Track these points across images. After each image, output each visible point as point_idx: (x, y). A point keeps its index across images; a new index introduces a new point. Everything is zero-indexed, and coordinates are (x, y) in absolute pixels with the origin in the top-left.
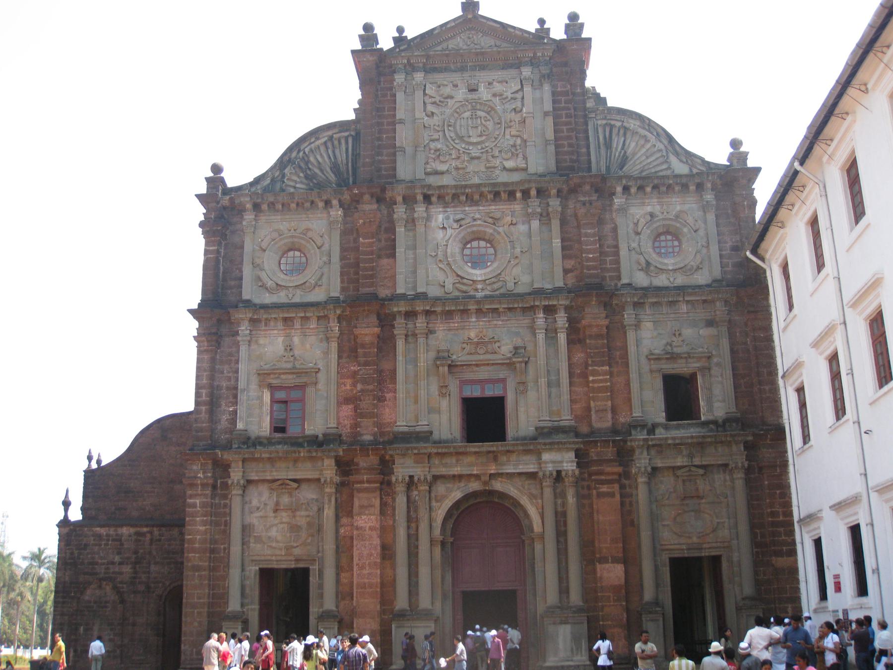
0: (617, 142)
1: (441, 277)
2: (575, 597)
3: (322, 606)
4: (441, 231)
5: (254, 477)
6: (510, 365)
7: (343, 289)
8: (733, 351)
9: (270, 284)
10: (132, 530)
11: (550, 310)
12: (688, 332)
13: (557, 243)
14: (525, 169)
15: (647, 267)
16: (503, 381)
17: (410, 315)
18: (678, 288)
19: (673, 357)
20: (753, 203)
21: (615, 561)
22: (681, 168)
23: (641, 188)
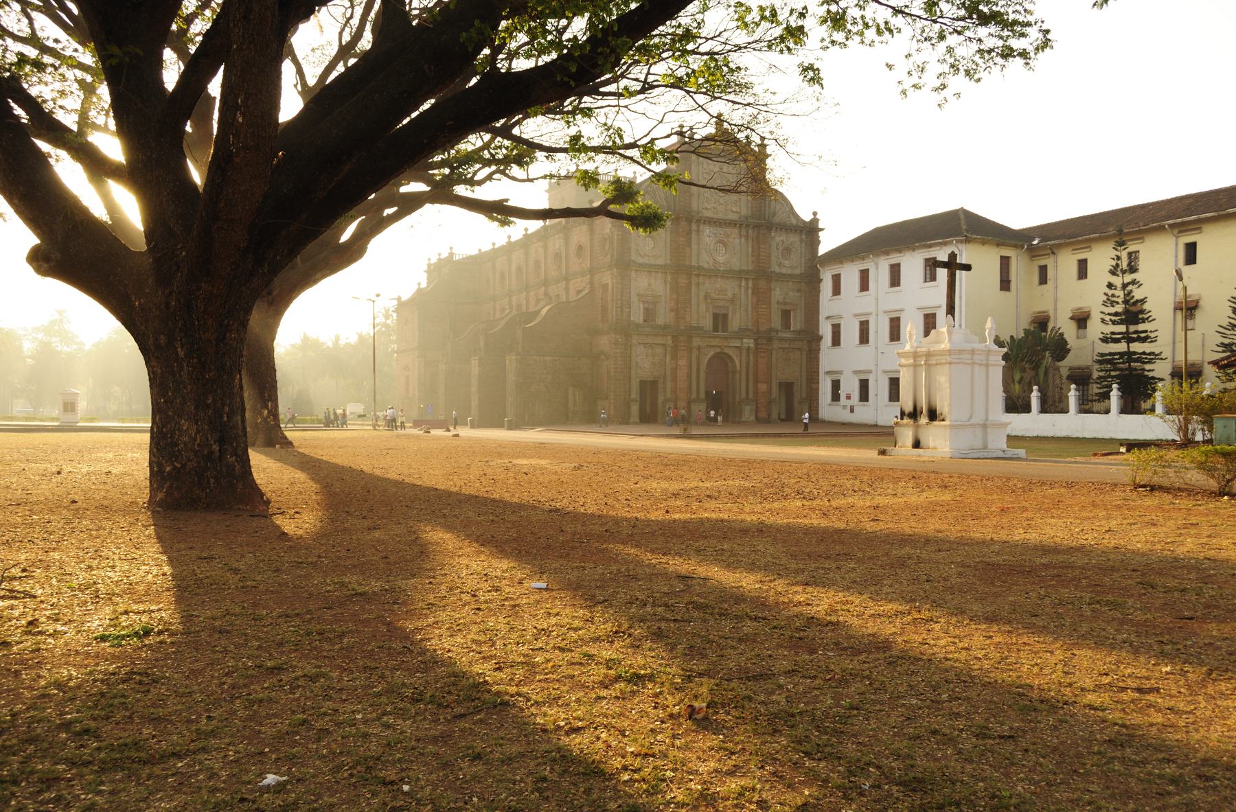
0: (773, 203)
1: (707, 259)
2: (751, 396)
3: (665, 396)
4: (708, 238)
5: (640, 341)
6: (732, 301)
7: (671, 260)
8: (805, 304)
9: (642, 254)
10: (551, 358)
11: (747, 279)
12: (791, 293)
13: (750, 249)
14: (739, 213)
15: (780, 265)
16: (728, 307)
17: (698, 275)
18: (790, 275)
19: (786, 304)
20: (819, 242)
21: (764, 382)
22: (794, 221)
23: (781, 229)
